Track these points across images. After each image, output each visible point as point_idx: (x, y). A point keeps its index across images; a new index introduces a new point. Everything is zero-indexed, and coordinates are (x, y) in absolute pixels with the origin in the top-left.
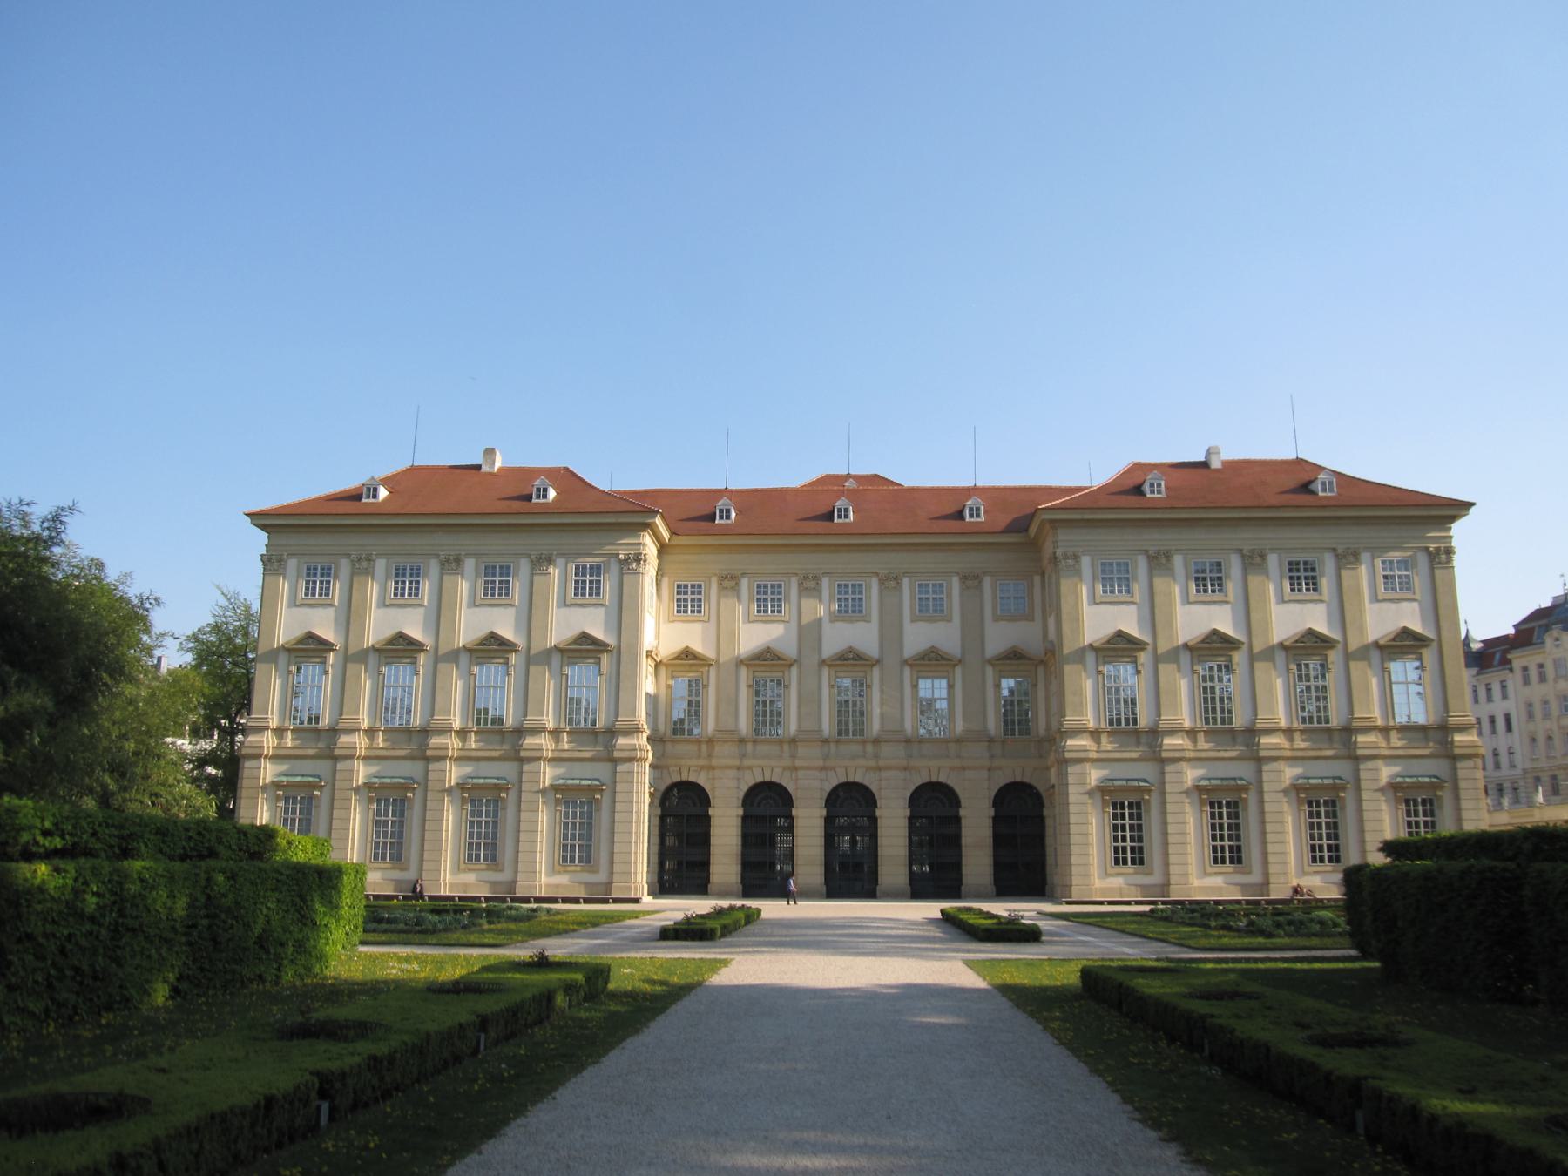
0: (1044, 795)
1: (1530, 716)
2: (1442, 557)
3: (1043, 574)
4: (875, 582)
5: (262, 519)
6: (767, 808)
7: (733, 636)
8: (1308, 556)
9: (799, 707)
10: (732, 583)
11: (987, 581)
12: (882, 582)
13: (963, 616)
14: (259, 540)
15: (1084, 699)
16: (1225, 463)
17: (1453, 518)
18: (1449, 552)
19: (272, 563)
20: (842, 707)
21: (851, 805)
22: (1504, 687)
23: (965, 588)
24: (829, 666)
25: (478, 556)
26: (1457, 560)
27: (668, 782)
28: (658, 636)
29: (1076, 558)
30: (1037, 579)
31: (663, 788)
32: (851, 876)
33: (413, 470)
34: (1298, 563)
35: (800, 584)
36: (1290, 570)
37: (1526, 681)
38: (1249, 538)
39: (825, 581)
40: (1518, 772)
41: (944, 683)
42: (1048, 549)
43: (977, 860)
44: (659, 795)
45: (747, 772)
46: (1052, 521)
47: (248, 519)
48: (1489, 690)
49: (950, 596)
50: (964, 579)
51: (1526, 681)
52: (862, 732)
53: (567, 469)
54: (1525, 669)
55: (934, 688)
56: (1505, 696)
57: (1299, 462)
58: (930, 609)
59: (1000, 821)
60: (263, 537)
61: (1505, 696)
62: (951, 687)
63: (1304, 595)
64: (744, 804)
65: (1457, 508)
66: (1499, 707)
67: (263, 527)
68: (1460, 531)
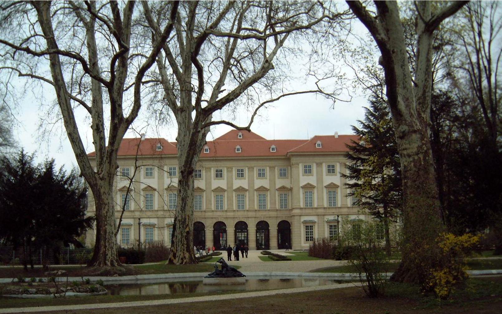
7: (210, 183)
11: (276, 168)
12: (249, 168)
13: (270, 176)
15: (300, 199)
16: (339, 136)
30: (289, 168)
35: (227, 169)
43: (274, 242)
50: (270, 167)
58: (261, 175)
59: (279, 231)
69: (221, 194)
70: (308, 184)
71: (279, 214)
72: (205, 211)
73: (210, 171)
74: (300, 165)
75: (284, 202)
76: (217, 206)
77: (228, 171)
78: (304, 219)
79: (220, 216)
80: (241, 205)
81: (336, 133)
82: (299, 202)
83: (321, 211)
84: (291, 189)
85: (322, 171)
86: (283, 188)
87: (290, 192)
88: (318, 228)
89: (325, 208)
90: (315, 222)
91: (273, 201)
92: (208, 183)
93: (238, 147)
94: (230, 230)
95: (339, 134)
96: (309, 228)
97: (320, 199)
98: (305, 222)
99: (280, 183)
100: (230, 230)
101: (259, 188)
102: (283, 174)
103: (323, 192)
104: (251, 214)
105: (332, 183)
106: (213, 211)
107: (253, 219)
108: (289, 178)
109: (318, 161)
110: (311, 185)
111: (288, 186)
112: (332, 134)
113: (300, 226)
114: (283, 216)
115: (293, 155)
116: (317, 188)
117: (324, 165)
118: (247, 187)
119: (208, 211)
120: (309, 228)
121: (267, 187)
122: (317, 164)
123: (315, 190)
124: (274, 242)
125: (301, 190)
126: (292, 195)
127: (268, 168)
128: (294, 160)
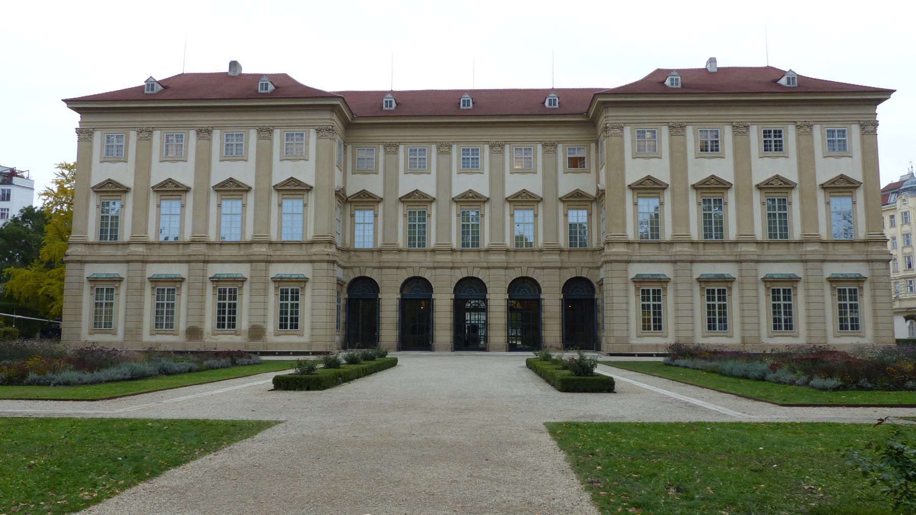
0: (596, 285)
2: (870, 127)
3: (597, 144)
4: (487, 147)
5: (74, 104)
6: (417, 295)
8: (777, 127)
9: (437, 228)
11: (560, 147)
12: (491, 147)
14: (75, 118)
16: (719, 69)
17: (880, 101)
18: (876, 124)
19: (84, 133)
20: (465, 229)
21: (470, 291)
23: (545, 153)
24: (456, 202)
25: (220, 127)
26: (880, 130)
27: (352, 277)
28: (345, 182)
29: (621, 128)
30: (593, 145)
31: (348, 280)
32: (468, 339)
33: (183, 74)
34: (770, 132)
36: (765, 137)
38: (738, 115)
39: (454, 147)
41: (531, 213)
42: (602, 123)
43: (552, 329)
44: (346, 285)
45: (404, 271)
46: (604, 103)
47: (65, 104)
50: (545, 145)
52: (478, 245)
55: (524, 216)
57: (769, 69)
60: (76, 117)
62: (536, 216)
63: (773, 153)
64: (401, 291)
65: (883, 94)
67: (77, 110)
68: (882, 110)
69: (422, 208)
70: (649, 178)
73: (396, 153)
74: (627, 130)
76: (411, 240)
77: (439, 153)
78: (636, 270)
79: (418, 264)
80: (470, 234)
81: (712, 61)
82: (624, 225)
83: (684, 250)
84: (601, 194)
85: (684, 145)
86: (576, 199)
87: (594, 206)
89: (693, 243)
90: (667, 281)
95: (720, 64)
96: (651, 293)
98: (639, 280)
99: (569, 182)
101: (518, 195)
103: (687, 202)
104: (495, 258)
105: (713, 177)
106: (400, 251)
107: (502, 271)
111: (592, 192)
112: (700, 63)
113: (627, 290)
114: (578, 266)
115: (607, 105)
116: (673, 191)
118: (485, 193)
119: (389, 251)
120: (651, 293)
122: (671, 128)
124: (552, 329)
126: (599, 213)
127: (539, 146)
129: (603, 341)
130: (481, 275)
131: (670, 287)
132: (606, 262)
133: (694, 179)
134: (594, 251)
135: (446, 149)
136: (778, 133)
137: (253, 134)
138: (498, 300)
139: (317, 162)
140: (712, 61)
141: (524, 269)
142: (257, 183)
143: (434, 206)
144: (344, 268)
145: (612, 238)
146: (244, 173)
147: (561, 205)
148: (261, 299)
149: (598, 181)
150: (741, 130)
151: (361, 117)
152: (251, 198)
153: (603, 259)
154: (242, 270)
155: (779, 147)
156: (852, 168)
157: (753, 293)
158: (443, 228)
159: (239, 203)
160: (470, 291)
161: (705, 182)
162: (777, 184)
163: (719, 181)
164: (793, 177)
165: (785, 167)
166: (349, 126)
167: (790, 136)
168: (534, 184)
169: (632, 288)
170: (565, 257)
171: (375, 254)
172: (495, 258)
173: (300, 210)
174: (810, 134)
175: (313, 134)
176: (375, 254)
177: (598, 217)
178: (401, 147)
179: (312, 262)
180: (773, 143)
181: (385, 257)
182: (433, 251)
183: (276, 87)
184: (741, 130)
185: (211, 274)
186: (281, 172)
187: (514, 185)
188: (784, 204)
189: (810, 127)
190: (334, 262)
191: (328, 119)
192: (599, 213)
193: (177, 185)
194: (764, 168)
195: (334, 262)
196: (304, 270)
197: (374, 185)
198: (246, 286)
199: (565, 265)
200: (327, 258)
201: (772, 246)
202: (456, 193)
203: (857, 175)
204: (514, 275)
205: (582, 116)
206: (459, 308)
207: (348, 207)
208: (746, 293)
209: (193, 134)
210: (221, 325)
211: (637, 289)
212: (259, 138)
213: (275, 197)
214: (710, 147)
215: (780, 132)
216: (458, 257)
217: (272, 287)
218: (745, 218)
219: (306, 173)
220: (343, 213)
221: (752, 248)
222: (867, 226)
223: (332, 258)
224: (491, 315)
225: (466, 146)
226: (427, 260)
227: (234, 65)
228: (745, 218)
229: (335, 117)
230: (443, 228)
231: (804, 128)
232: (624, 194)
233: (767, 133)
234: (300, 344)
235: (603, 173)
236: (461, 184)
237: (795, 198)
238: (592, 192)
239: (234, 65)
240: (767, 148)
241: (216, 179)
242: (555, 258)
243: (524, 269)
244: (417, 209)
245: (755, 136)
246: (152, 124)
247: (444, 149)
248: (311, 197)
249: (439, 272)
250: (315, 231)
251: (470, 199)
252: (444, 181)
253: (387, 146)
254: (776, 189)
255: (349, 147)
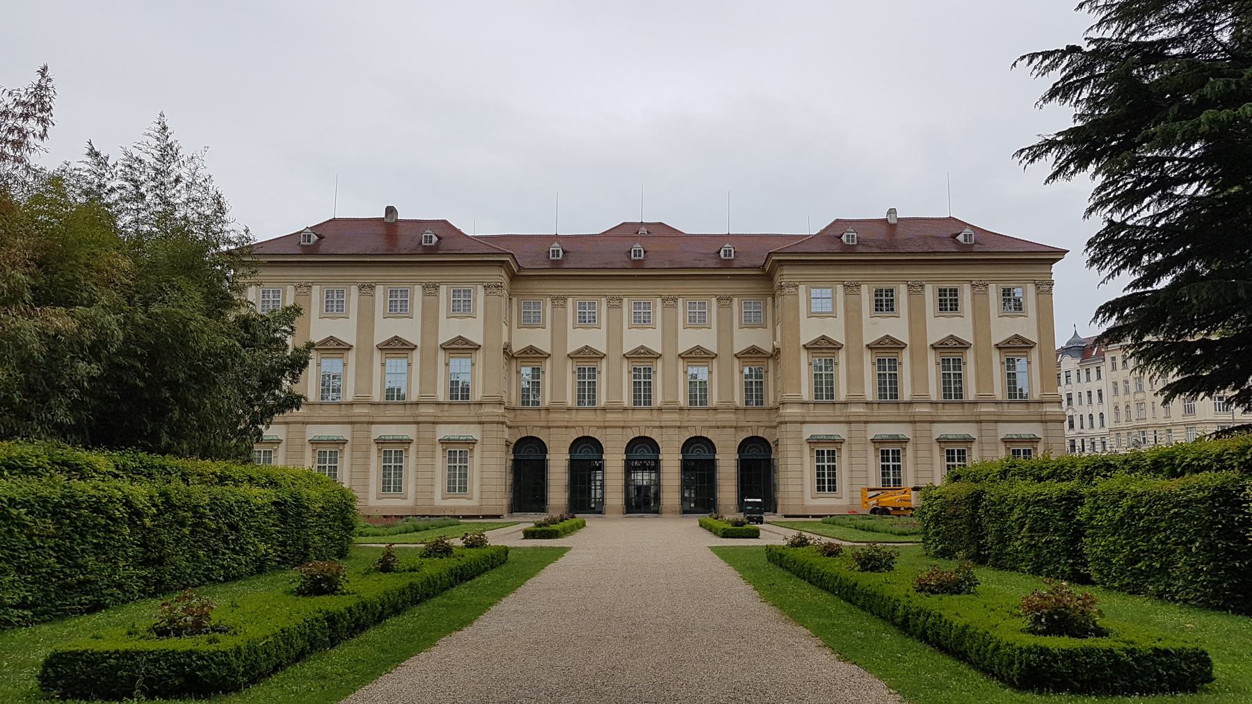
1: (1116, 390)
2: (1044, 288)
6: (586, 458)
8: (953, 286)
10: (561, 302)
11: (736, 300)
17: (1056, 260)
18: (1051, 284)
22: (1099, 372)
28: (510, 338)
30: (769, 299)
32: (642, 502)
37: (1114, 368)
38: (913, 273)
40: (1106, 430)
48: (1088, 373)
49: (710, 311)
51: (1114, 368)
53: (445, 221)
54: (1114, 358)
56: (1099, 378)
61: (1099, 378)
62: (710, 373)
63: (948, 313)
66: (1094, 386)
71: (742, 419)
72: (547, 409)
75: (754, 391)
78: (809, 431)
80: (642, 393)
81: (892, 211)
82: (799, 385)
84: (776, 354)
85: (859, 305)
86: (753, 353)
87: (771, 362)
88: (850, 457)
91: (724, 386)
92: (559, 336)
93: (638, 246)
94: (614, 460)
96: (826, 457)
97: (855, 379)
98: (813, 441)
99: (744, 339)
100: (614, 460)
102: (752, 322)
106: (569, 409)
108: (770, 324)
109: (847, 280)
110: (830, 341)
113: (801, 451)
114: (755, 425)
117: (864, 288)
119: (558, 410)
120: (826, 457)
121: (712, 347)
123: (842, 355)
125: (804, 355)
126: (776, 370)
127: (714, 299)
128: (786, 276)
129: (780, 502)
130: (654, 435)
131: (844, 448)
132: (781, 423)
133: (869, 339)
134: (770, 409)
135: (617, 303)
136: (954, 292)
137: (418, 290)
138: (671, 462)
139: (485, 320)
140: (892, 211)
141: (699, 428)
142: (422, 341)
143: (604, 361)
144: (510, 427)
145: (787, 399)
146: (409, 330)
147: (736, 361)
148: (429, 461)
149: (775, 339)
150: (915, 289)
151: (528, 267)
152: (416, 355)
153: (778, 420)
154: (408, 432)
155: (955, 306)
156: (1025, 326)
157: (926, 454)
158: (615, 386)
159: (405, 362)
160: (643, 452)
161: (879, 342)
162: (951, 344)
163: (894, 341)
164: (968, 337)
165: (960, 326)
166: (514, 277)
167: (966, 294)
168: (707, 339)
169: (807, 448)
170: (741, 415)
171: (543, 412)
172: (667, 417)
173: (468, 369)
174: (986, 293)
175: (480, 289)
176: (543, 412)
177: (775, 375)
178: (570, 300)
179: (480, 423)
180: (948, 302)
181: (553, 416)
182: (604, 409)
183: (440, 238)
184: (915, 289)
185: (375, 436)
186: (449, 330)
187: (688, 339)
188: (959, 363)
189: (986, 286)
190: (503, 423)
191: (499, 276)
192: (776, 370)
193: (339, 343)
194: (939, 327)
195: (503, 423)
196: (473, 432)
197: (541, 339)
198: (412, 448)
199: (740, 424)
200: (497, 419)
201: (946, 406)
202: (627, 349)
203: (1031, 335)
204: (687, 435)
205: (759, 268)
206: (629, 468)
207: (514, 363)
208: (920, 454)
209: (354, 290)
210: (386, 487)
211: (812, 450)
212: (424, 295)
213: (441, 355)
214: (884, 303)
215: (956, 290)
216: (630, 416)
217: (439, 448)
218: (920, 378)
219: (473, 330)
220: (509, 370)
221: (925, 409)
222: (1042, 386)
223: (501, 419)
224: (664, 476)
225: (638, 300)
226: (599, 417)
227: (390, 210)
228: (920, 378)
229: (503, 273)
230: (615, 386)
231: (980, 288)
232: (799, 353)
233: (942, 292)
234: (468, 508)
235: (778, 328)
236: (633, 339)
237: (970, 356)
238: (770, 351)
239: (390, 210)
240: (942, 307)
241: (380, 338)
242: (730, 417)
243: (699, 428)
244: (587, 365)
245: (930, 295)
246: (311, 279)
247: (615, 302)
248: (479, 355)
249: (609, 431)
250: (484, 392)
251: (642, 356)
252: (614, 336)
253: (554, 299)
254: (951, 350)
255: (515, 299)
